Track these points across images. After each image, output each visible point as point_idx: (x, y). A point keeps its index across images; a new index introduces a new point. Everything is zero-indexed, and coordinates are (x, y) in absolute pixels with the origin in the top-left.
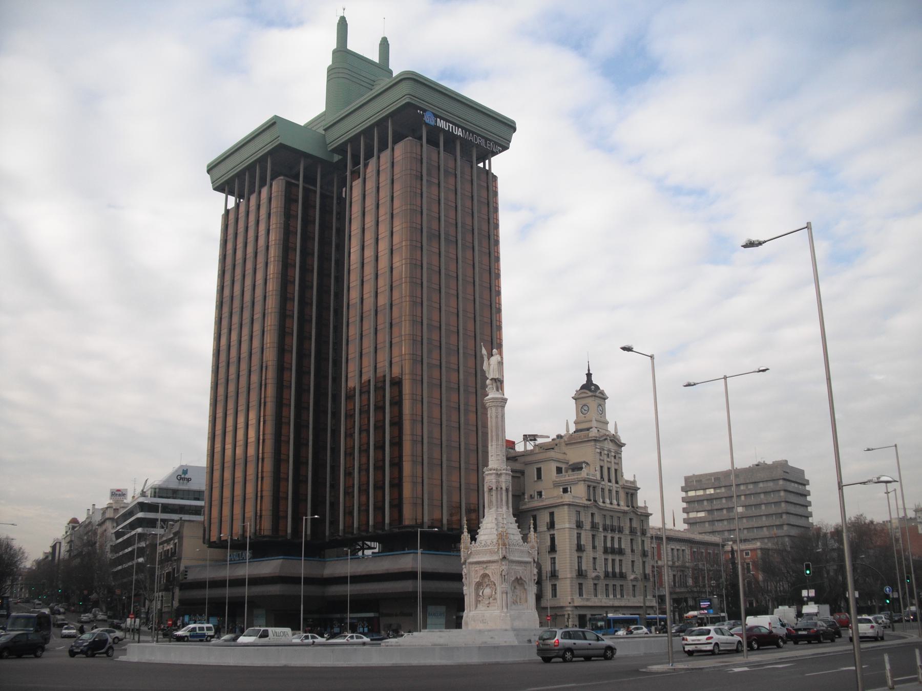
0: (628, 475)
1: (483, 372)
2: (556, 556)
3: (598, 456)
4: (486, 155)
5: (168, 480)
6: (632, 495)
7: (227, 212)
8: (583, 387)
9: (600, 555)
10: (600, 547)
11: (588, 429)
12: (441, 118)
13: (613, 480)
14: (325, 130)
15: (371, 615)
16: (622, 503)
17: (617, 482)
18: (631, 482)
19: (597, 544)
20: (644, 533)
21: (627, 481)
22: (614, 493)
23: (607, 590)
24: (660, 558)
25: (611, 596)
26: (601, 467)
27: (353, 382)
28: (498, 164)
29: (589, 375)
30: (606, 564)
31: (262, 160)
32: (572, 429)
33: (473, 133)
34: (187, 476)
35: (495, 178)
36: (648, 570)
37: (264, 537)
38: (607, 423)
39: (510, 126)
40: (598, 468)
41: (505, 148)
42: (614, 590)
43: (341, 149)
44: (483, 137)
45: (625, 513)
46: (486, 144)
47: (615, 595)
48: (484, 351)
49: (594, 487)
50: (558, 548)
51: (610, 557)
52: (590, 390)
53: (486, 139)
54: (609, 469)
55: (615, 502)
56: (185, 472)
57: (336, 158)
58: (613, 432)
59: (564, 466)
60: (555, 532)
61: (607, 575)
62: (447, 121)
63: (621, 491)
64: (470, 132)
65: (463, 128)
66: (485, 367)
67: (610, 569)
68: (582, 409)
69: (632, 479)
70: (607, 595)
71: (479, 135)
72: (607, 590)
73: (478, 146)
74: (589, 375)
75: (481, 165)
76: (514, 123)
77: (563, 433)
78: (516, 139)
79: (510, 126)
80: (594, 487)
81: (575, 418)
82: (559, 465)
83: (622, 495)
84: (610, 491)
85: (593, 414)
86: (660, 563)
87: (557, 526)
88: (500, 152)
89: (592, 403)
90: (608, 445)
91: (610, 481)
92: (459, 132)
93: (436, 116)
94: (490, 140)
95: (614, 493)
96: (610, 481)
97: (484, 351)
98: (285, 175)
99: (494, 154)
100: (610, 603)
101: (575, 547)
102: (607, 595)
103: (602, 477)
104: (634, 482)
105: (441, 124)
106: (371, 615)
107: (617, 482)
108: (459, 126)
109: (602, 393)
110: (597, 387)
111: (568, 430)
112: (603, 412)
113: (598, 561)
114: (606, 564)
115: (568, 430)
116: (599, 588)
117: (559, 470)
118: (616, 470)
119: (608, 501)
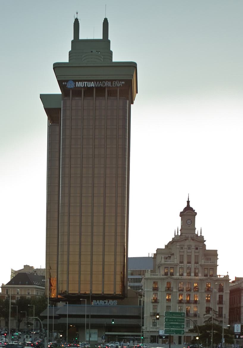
12: (78, 81)
29: (188, 202)
33: (102, 81)
44: (109, 80)
46: (112, 84)
53: (112, 81)
63: (200, 267)
64: (99, 81)
71: (105, 80)
74: (188, 202)
90: (193, 244)
92: (92, 84)
93: (75, 81)
94: (115, 80)
105: (79, 84)
107: (196, 263)
108: (91, 81)
110: (192, 209)
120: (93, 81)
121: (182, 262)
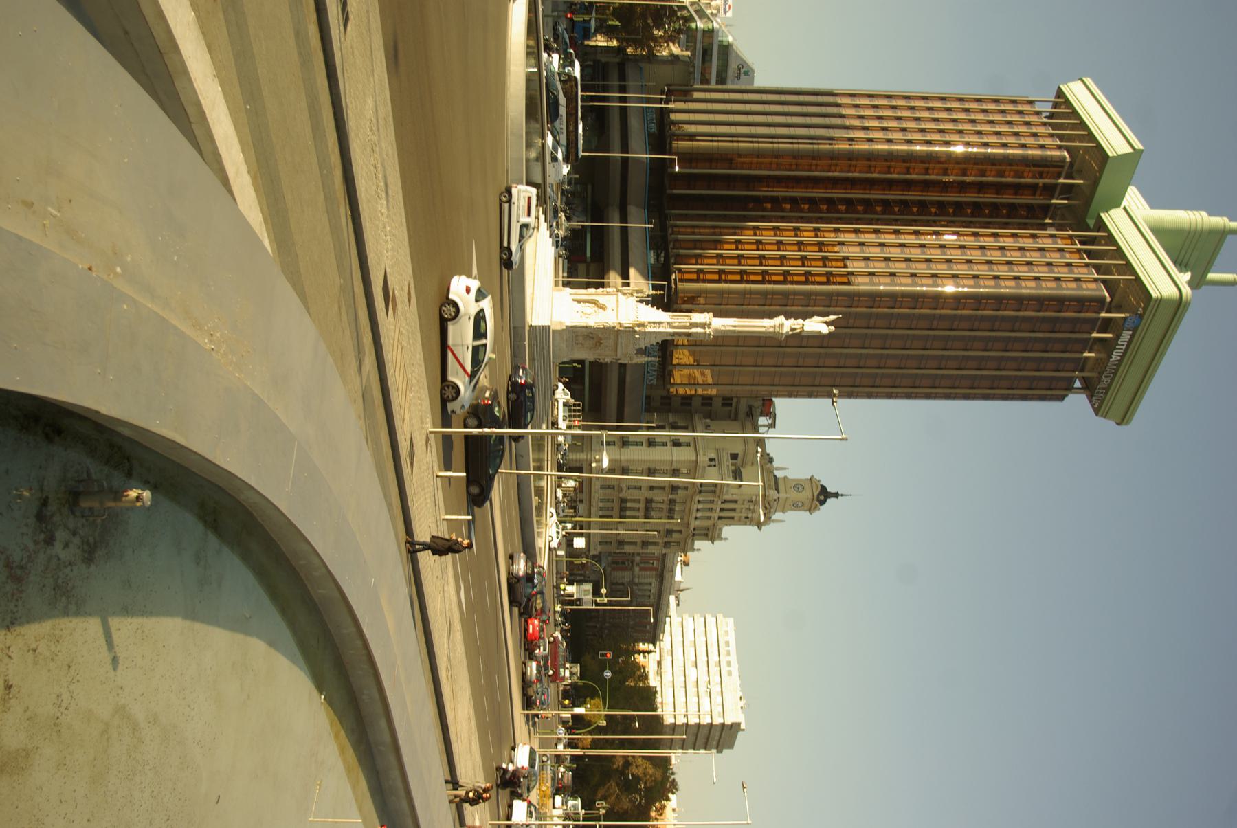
0: (728, 531)
1: (811, 316)
2: (644, 447)
3: (747, 498)
4: (1089, 388)
5: (738, 56)
6: (707, 535)
7: (1031, 103)
8: (823, 489)
9: (643, 495)
10: (650, 495)
11: (777, 489)
12: (1132, 336)
13: (722, 514)
14: (1125, 209)
15: (588, 254)
16: (698, 523)
17: (720, 518)
18: (719, 535)
19: (655, 491)
20: (667, 545)
21: (721, 530)
22: (709, 514)
23: (608, 501)
24: (642, 569)
25: (601, 505)
26: (736, 502)
27: (830, 238)
28: (1077, 402)
29: (836, 495)
30: (634, 501)
31: (1091, 137)
32: (779, 474)
34: (742, 76)
35: (1061, 398)
36: (628, 549)
37: (670, 144)
38: (784, 512)
39: (1124, 419)
40: (735, 497)
41: (1097, 411)
42: (608, 509)
43: (1101, 226)
44: (1110, 386)
45: (688, 524)
47: (601, 509)
48: (832, 317)
49: (714, 492)
50: (652, 449)
51: (642, 506)
52: (820, 494)
53: (1107, 389)
54: (734, 510)
55: (699, 515)
56: (746, 73)
57: (1091, 222)
58: (774, 517)
59: (739, 461)
60: (669, 447)
61: (623, 501)
62: (1130, 342)
63: (711, 522)
64: (1116, 371)
65: (1120, 361)
66: (816, 318)
67: (629, 505)
68: (798, 486)
69: (723, 536)
70: (602, 501)
72: (608, 501)
73: (1099, 380)
74: (836, 495)
75: (1077, 384)
76: (1128, 423)
77: (775, 464)
78: (1108, 425)
79: (1123, 419)
80: (714, 492)
81: (791, 476)
82: (740, 457)
83: (706, 523)
84: (711, 510)
85: (794, 495)
86: (637, 569)
87: (675, 449)
88: (1093, 406)
89: (806, 495)
91: (722, 510)
92: (1115, 357)
93: (1135, 330)
94: (1106, 394)
95: (709, 514)
96: (722, 510)
97: (832, 317)
98: (1071, 164)
99: (1090, 398)
100: (594, 503)
101: (652, 466)
102: (602, 501)
103: (724, 502)
104: (720, 538)
105: (1126, 336)
106: (588, 254)
107: (720, 518)
108: (1123, 357)
109: (816, 508)
110: (822, 503)
111: (778, 469)
112: (796, 506)
113: (637, 491)
114: (634, 501)
115: (778, 469)
116: (610, 491)
117: (734, 456)
118: (732, 518)
119: (700, 506)
120: (1120, 361)
121: (724, 502)
